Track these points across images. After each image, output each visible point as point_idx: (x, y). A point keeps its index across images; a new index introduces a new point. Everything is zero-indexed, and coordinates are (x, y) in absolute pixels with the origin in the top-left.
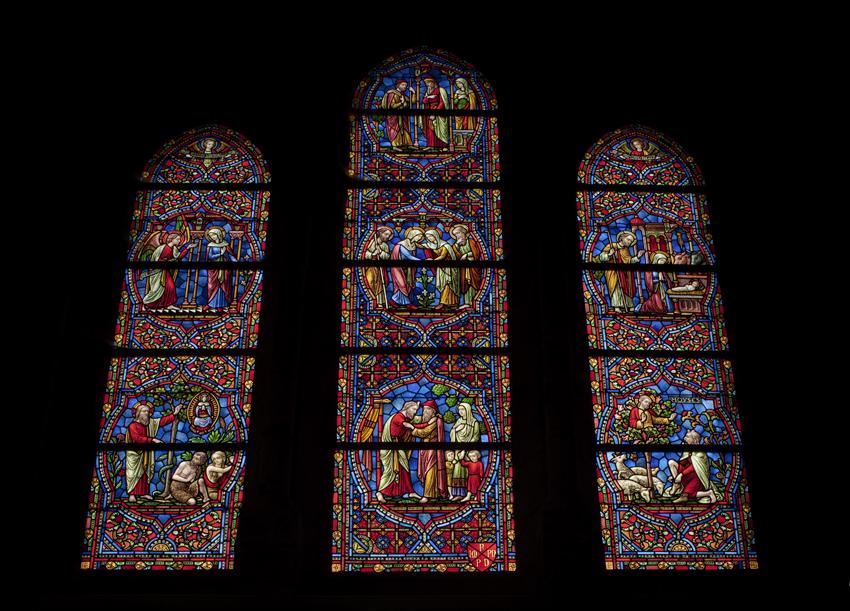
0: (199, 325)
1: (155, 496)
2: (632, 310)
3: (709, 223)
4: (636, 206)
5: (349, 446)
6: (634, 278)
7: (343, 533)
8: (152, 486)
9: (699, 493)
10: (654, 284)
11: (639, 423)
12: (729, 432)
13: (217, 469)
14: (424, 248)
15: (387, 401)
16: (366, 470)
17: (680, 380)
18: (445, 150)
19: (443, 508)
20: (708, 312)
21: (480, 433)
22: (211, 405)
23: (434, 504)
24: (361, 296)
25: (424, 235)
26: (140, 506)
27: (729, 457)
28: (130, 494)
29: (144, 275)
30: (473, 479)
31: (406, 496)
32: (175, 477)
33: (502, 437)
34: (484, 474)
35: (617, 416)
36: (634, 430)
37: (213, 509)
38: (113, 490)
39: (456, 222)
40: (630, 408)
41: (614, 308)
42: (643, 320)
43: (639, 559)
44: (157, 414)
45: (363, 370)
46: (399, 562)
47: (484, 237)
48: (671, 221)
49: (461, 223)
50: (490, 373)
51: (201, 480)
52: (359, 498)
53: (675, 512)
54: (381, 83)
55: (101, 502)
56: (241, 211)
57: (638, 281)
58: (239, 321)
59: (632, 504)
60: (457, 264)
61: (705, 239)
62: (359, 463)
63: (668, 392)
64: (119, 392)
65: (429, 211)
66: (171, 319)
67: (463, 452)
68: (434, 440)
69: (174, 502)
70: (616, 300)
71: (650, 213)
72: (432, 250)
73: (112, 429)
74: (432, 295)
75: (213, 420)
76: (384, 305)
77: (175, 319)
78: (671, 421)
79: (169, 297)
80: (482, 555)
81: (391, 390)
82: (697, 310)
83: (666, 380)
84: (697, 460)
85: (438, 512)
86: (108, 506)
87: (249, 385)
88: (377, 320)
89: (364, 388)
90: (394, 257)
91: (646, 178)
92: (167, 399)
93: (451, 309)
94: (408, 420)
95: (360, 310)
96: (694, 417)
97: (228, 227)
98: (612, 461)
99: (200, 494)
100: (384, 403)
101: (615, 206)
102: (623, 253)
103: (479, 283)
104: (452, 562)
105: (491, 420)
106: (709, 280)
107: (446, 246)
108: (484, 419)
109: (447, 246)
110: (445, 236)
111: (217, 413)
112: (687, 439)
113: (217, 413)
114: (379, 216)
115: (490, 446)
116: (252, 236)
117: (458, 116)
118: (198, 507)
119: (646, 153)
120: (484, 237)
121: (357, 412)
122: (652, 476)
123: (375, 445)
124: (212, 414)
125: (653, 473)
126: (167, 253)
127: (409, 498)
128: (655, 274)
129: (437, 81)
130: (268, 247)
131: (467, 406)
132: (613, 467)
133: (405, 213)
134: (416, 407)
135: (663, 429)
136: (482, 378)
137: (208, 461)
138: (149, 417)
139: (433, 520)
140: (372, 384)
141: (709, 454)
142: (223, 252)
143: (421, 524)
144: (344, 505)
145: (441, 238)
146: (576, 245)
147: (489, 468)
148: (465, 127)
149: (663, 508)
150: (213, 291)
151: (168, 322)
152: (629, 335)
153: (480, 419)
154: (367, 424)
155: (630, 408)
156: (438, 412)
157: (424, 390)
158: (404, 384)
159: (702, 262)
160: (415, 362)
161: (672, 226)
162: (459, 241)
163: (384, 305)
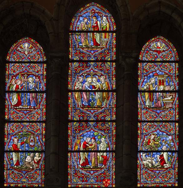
0: (29, 112)
1: (21, 166)
2: (152, 106)
4: (156, 68)
5: (71, 152)
6: (153, 95)
7: (71, 176)
8: (20, 163)
9: (165, 165)
10: (159, 97)
11: (150, 143)
12: (175, 146)
13: (37, 158)
14: (92, 85)
15: (82, 137)
17: (163, 130)
18: (99, 47)
19: (97, 169)
20: (174, 107)
22: (34, 139)
23: (94, 168)
25: (92, 80)
26: (18, 169)
27: (174, 154)
28: (15, 165)
29: (11, 95)
31: (87, 166)
32: (26, 160)
33: (113, 149)
35: (144, 142)
36: (149, 146)
37: (37, 170)
38: (10, 164)
39: (102, 75)
40: (148, 139)
41: (146, 106)
42: (154, 110)
43: (147, 184)
44: (19, 141)
45: (75, 127)
46: (85, 184)
47: (110, 80)
48: (167, 74)
49: (103, 75)
51: (33, 161)
52: (75, 167)
53: (157, 170)
54: (79, 19)
55: (7, 168)
56: (38, 72)
57: (154, 96)
58: (40, 111)
59: (146, 168)
60: (103, 91)
61: (176, 80)
62: (74, 156)
63: (159, 134)
64: (8, 134)
65: (94, 71)
66: (21, 110)
67: (102, 153)
68: (94, 150)
69: (26, 168)
70: (147, 104)
71: (160, 71)
72: (94, 86)
73: (8, 146)
74: (94, 102)
75: (35, 143)
76: (80, 105)
77: (22, 110)
78: (159, 143)
79: (19, 103)
80: (106, 182)
81: (83, 134)
82: (171, 106)
83: (159, 130)
84: (165, 155)
85: (95, 170)
86: (9, 169)
87: (44, 132)
88: (79, 111)
89: (75, 133)
90: (83, 89)
91: (161, 57)
92: (22, 136)
94: (87, 143)
95: (74, 107)
96: (166, 142)
97: (34, 77)
98: (142, 156)
99: (33, 165)
101: (150, 68)
102: (151, 86)
103: (108, 98)
104: (98, 184)
106: (175, 95)
108: (108, 143)
110: (99, 81)
111: (36, 141)
112: (163, 148)
113: (36, 141)
114: (79, 73)
115: (109, 151)
116: (42, 81)
117: (103, 33)
118: (33, 169)
119: (161, 48)
120: (110, 80)
121: (74, 141)
123: (79, 151)
124: (35, 141)
125: (153, 159)
126: (17, 87)
127: (88, 167)
128: (160, 93)
129: (97, 18)
130: (46, 85)
131: (103, 139)
132: (142, 157)
133: (87, 72)
134: (90, 139)
135: (157, 146)
136: (108, 130)
137: (34, 156)
138: (18, 142)
140: (78, 132)
141: (169, 153)
142: (33, 87)
143: (91, 174)
144: (71, 169)
145: (97, 81)
146: (137, 83)
147: (109, 158)
148: (105, 37)
150: (32, 101)
151: (20, 111)
152: (150, 115)
153: (107, 143)
154: (76, 144)
155: (148, 139)
156: (96, 141)
157: (92, 134)
158: (87, 132)
159: (174, 89)
160: (89, 125)
162: (102, 82)
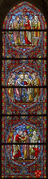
7: (4, 167)
16: (10, 150)
19: (29, 161)
21: (38, 140)
23: (26, 160)
24: (7, 98)
25: (24, 77)
30: (37, 152)
31: (19, 158)
33: (44, 141)
34: (39, 151)
39: (33, 72)
45: (8, 121)
46: (18, 175)
50: (41, 122)
52: (8, 158)
65: (26, 68)
67: (34, 145)
76: (13, 101)
80: (38, 173)
85: (27, 162)
93: (31, 102)
94: (20, 136)
95: (7, 102)
100: (14, 131)
103: (39, 93)
104: (30, 175)
105: (41, 136)
107: (30, 81)
109: (30, 80)
110: (30, 77)
117: (35, 31)
121: (7, 134)
127: (20, 158)
129: (28, 17)
133: (19, 69)
134: (22, 132)
139: (26, 164)
140: (11, 125)
144: (4, 160)
147: (40, 150)
148: (37, 36)
154: (9, 137)
156: (27, 134)
157: (24, 127)
160: (22, 119)
162: (34, 79)
163: (13, 101)
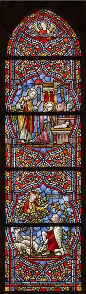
2: (31, 141)
3: (80, 81)
9: (56, 250)
17: (53, 184)
35: (17, 207)
40: (25, 201)
41: (21, 140)
42: (36, 147)
43: (22, 286)
57: (35, 123)
82: (67, 140)
84: (57, 231)
106: (75, 120)
112: (53, 219)
119: (48, 31)
122: (33, 241)
125: (34, 239)
128: (45, 117)
132: (13, 236)
135: (41, 214)
141: (63, 228)
149: (36, 258)
155: (25, 201)
161: (58, 84)
